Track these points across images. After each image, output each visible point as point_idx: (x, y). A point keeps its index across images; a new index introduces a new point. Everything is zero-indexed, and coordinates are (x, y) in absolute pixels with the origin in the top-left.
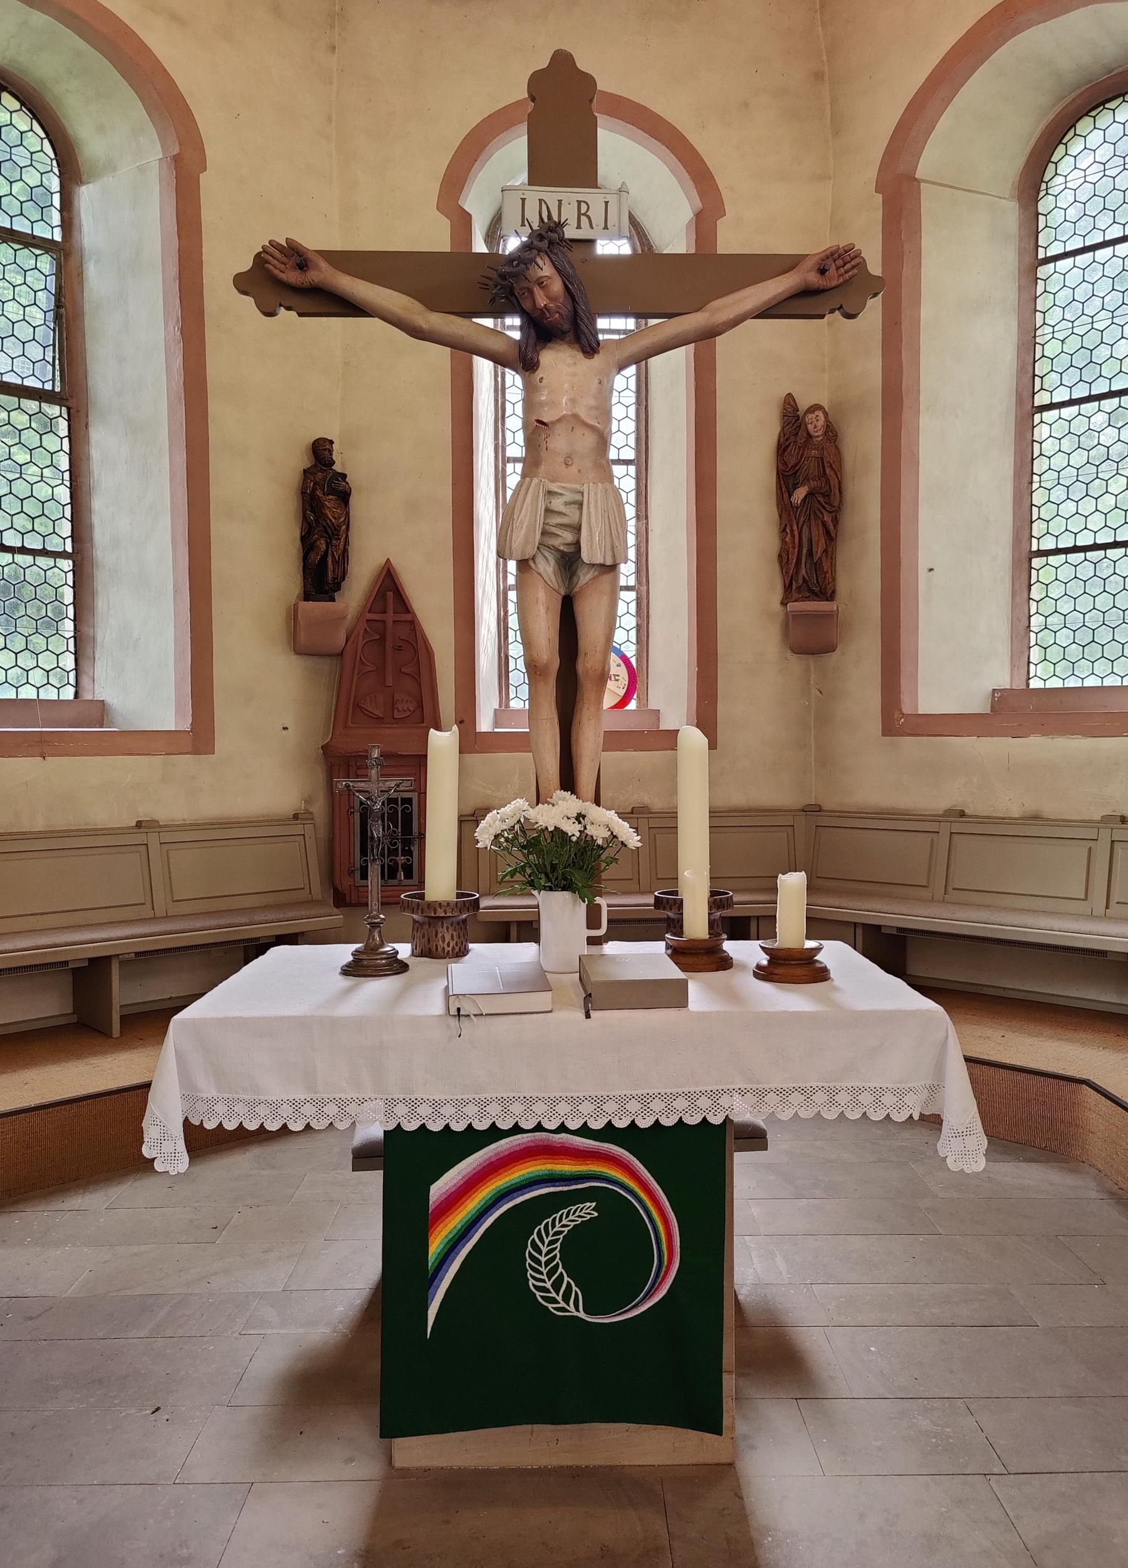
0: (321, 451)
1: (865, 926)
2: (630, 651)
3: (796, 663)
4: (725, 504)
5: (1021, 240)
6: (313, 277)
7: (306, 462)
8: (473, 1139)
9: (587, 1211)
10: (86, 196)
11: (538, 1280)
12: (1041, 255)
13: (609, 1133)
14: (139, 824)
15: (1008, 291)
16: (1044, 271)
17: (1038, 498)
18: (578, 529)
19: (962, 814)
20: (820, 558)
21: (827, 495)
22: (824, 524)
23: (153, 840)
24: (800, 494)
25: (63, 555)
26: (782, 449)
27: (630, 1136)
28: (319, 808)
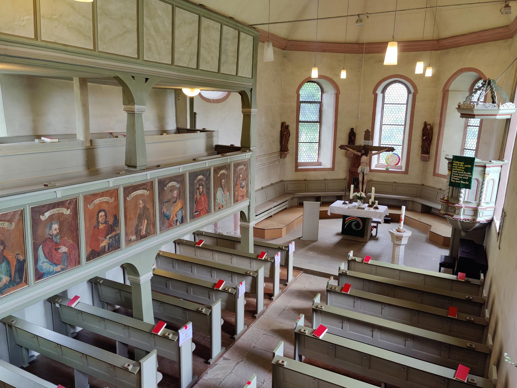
0: (352, 130)
1: (422, 204)
2: (400, 155)
4: (413, 138)
6: (345, 148)
7: (350, 131)
8: (349, 216)
9: (356, 222)
10: (324, 95)
11: (352, 226)
13: (358, 217)
14: (325, 180)
17: (467, 140)
18: (364, 171)
19: (441, 189)
21: (429, 138)
22: (428, 143)
24: (425, 138)
25: (318, 142)
26: (423, 130)
27: (359, 218)
28: (348, 178)
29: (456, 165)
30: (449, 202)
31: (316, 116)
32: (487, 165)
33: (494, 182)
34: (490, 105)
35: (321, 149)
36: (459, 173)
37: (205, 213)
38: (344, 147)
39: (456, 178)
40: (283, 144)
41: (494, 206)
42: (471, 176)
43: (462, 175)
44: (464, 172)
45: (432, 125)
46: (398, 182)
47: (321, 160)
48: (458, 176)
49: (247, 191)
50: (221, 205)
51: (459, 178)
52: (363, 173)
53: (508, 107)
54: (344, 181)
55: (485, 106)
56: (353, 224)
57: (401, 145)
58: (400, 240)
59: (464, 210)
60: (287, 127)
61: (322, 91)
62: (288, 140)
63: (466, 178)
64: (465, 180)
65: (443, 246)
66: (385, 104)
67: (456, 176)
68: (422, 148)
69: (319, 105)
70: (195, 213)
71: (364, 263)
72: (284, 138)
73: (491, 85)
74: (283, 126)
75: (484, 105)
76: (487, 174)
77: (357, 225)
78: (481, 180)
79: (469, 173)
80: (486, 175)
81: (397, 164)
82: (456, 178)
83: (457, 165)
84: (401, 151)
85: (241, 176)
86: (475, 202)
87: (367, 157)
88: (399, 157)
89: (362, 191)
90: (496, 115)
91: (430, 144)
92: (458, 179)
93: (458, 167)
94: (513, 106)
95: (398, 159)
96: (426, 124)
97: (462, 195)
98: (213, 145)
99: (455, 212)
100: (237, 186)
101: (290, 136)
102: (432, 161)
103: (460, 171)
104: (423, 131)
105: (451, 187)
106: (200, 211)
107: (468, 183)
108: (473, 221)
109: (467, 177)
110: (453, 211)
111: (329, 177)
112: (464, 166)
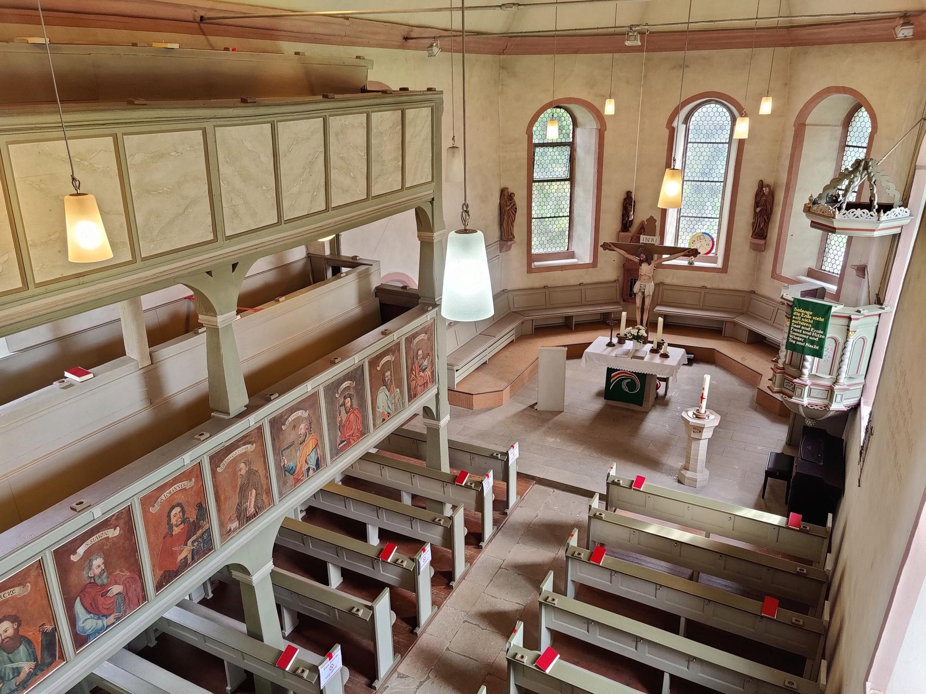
0: (629, 194)
2: (715, 236)
3: (753, 253)
4: (738, 208)
5: (841, 139)
6: (611, 248)
8: (617, 370)
10: (579, 131)
11: (623, 387)
12: (847, 144)
13: (632, 372)
14: (580, 284)
15: (834, 154)
16: (847, 149)
20: (762, 227)
23: (583, 287)
25: (567, 216)
26: (757, 195)
27: (635, 373)
29: (799, 314)
30: (786, 372)
31: (564, 169)
32: (852, 317)
33: (864, 342)
34: (864, 213)
35: (574, 228)
36: (803, 330)
37: (358, 438)
38: (610, 246)
39: (798, 337)
40: (505, 228)
41: (864, 381)
42: (823, 337)
43: (809, 333)
44: (812, 329)
45: (772, 185)
46: (709, 286)
47: (574, 248)
48: (802, 333)
49: (432, 373)
50: (386, 413)
51: (802, 338)
52: (643, 293)
53: (897, 216)
54: (615, 284)
55: (855, 215)
56: (624, 383)
57: (716, 218)
58: (700, 432)
59: (810, 389)
60: (511, 197)
61: (575, 124)
62: (513, 221)
63: (816, 339)
64: (812, 343)
65: (779, 416)
66: (690, 142)
67: (798, 334)
68: (753, 227)
69: (568, 148)
70: (339, 444)
71: (634, 489)
72: (506, 217)
73: (869, 171)
74: (504, 195)
75: (853, 212)
76: (852, 331)
77: (631, 385)
78: (841, 340)
79: (820, 332)
80: (850, 333)
81: (709, 252)
82: (798, 337)
83: (801, 315)
84: (716, 228)
85: (420, 352)
86: (830, 377)
87: (650, 266)
88: (712, 239)
89: (642, 324)
90: (874, 230)
91: (769, 221)
92: (800, 339)
93: (801, 319)
94: (906, 212)
95: (711, 243)
96: (761, 184)
97: (807, 364)
98: (370, 289)
99: (794, 390)
100: (414, 373)
101: (516, 212)
102: (770, 255)
103: (805, 326)
104: (756, 197)
105: (789, 351)
106: (349, 439)
107: (817, 348)
108: (825, 407)
109: (816, 337)
110: (790, 388)
111: (587, 280)
112: (812, 318)
